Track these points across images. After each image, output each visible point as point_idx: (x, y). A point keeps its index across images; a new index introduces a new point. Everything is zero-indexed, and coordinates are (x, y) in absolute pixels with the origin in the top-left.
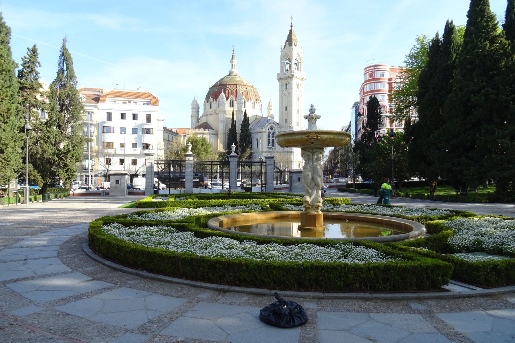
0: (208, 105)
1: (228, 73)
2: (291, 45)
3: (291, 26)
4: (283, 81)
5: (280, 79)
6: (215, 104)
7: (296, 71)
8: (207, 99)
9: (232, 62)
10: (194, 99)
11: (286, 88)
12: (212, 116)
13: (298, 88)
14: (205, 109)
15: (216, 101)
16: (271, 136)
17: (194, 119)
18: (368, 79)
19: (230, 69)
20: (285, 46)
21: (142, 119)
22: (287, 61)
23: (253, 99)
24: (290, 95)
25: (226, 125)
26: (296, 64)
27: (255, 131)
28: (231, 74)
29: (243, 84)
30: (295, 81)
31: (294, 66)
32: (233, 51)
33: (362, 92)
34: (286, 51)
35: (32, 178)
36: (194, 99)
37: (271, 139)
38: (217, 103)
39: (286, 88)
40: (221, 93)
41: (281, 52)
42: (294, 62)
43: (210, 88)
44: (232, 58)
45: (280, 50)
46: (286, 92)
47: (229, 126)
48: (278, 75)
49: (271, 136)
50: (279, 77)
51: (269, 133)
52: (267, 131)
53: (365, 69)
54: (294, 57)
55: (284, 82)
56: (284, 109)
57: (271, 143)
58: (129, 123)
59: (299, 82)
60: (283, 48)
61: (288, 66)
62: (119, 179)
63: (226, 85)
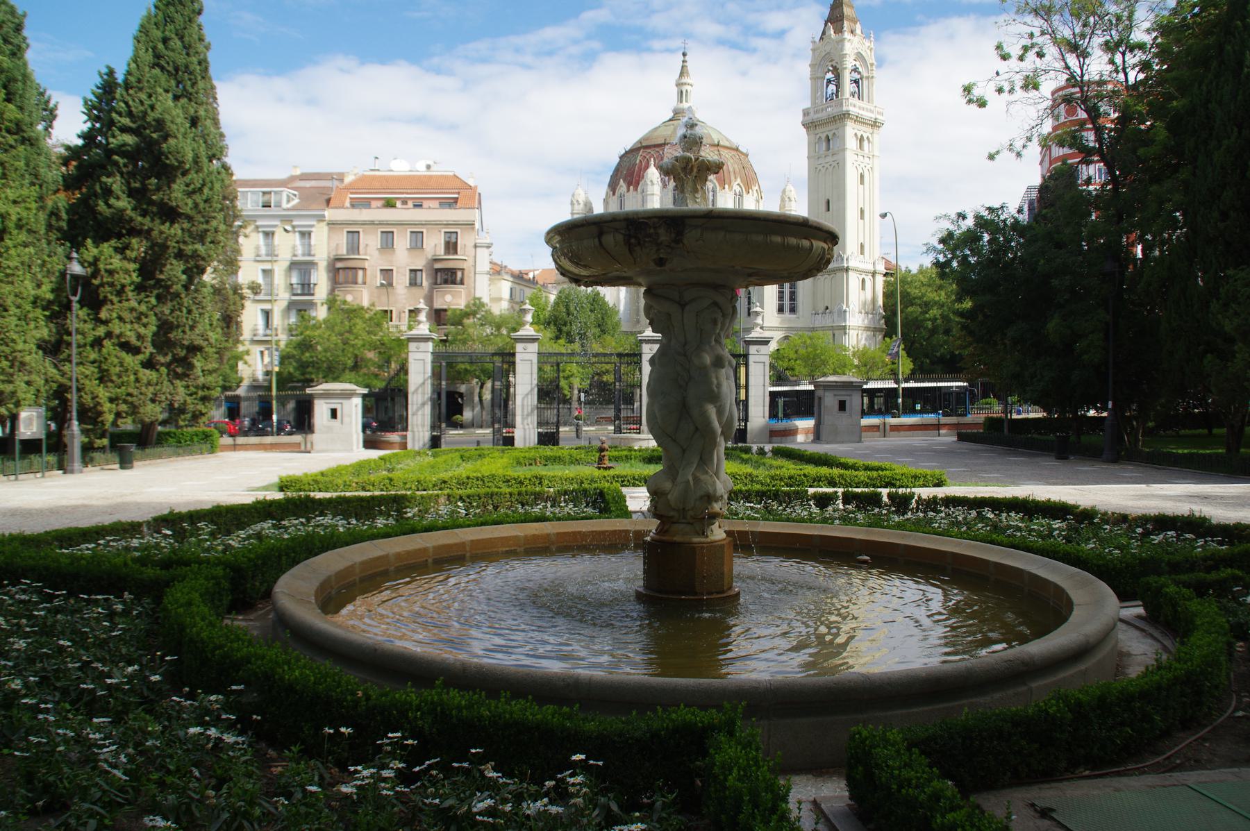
1: (671, 115)
2: (839, 30)
4: (818, 131)
5: (810, 125)
7: (855, 101)
8: (613, 186)
9: (679, 85)
11: (828, 149)
13: (861, 147)
15: (636, 189)
19: (674, 102)
20: (824, 33)
21: (434, 244)
22: (830, 75)
23: (739, 181)
24: (838, 168)
26: (856, 82)
28: (677, 113)
30: (851, 130)
31: (848, 88)
32: (684, 55)
33: (1047, 158)
34: (828, 49)
35: (87, 399)
39: (828, 149)
40: (647, 166)
41: (814, 50)
42: (847, 77)
43: (621, 157)
44: (682, 74)
45: (811, 46)
46: (829, 159)
48: (806, 113)
50: (809, 119)
53: (1053, 93)
54: (849, 63)
55: (823, 132)
56: (824, 207)
57: (787, 302)
58: (403, 259)
59: (865, 131)
60: (817, 39)
61: (832, 87)
62: (338, 407)
63: (665, 144)
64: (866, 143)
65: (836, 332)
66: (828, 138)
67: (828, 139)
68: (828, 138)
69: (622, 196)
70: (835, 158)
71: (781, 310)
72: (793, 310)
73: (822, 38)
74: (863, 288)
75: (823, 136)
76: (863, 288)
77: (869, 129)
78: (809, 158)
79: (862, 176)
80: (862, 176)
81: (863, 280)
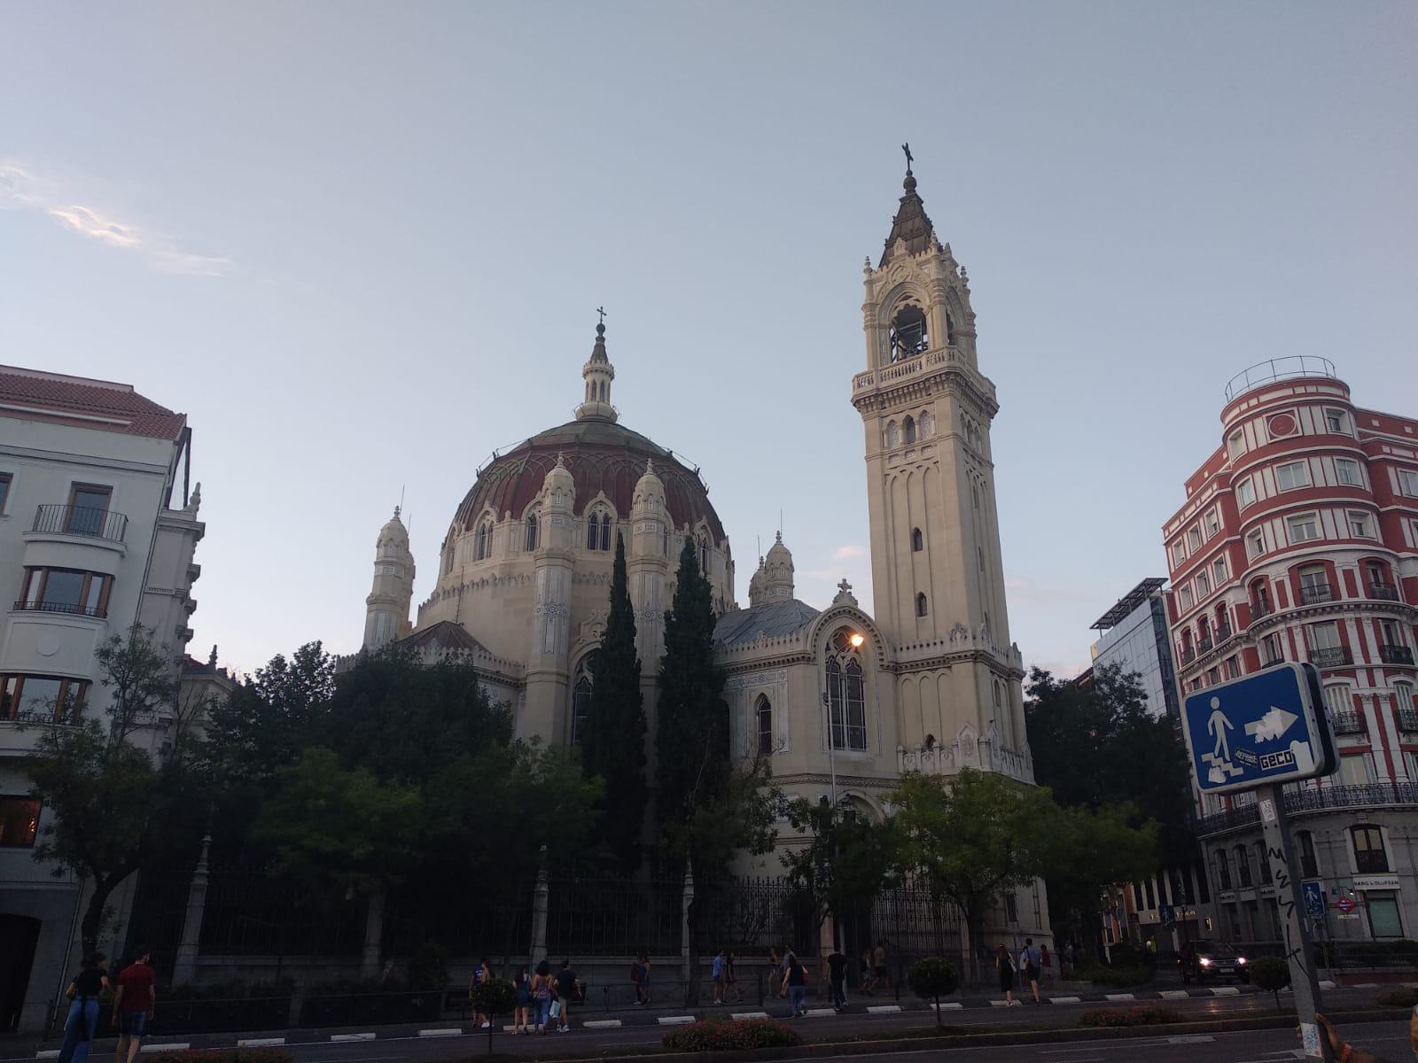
0: (466, 546)
3: (910, 184)
6: (506, 535)
8: (468, 513)
10: (397, 519)
11: (909, 438)
12: (488, 590)
14: (448, 566)
17: (382, 616)
18: (1263, 442)
25: (574, 630)
27: (748, 656)
32: (601, 328)
36: (397, 519)
38: (522, 528)
41: (870, 283)
45: (865, 277)
47: (593, 636)
50: (867, 388)
52: (822, 659)
60: (875, 266)
64: (973, 436)
66: (909, 423)
67: (909, 423)
69: (484, 535)
70: (929, 453)
72: (859, 742)
73: (885, 261)
77: (976, 415)
78: (868, 459)
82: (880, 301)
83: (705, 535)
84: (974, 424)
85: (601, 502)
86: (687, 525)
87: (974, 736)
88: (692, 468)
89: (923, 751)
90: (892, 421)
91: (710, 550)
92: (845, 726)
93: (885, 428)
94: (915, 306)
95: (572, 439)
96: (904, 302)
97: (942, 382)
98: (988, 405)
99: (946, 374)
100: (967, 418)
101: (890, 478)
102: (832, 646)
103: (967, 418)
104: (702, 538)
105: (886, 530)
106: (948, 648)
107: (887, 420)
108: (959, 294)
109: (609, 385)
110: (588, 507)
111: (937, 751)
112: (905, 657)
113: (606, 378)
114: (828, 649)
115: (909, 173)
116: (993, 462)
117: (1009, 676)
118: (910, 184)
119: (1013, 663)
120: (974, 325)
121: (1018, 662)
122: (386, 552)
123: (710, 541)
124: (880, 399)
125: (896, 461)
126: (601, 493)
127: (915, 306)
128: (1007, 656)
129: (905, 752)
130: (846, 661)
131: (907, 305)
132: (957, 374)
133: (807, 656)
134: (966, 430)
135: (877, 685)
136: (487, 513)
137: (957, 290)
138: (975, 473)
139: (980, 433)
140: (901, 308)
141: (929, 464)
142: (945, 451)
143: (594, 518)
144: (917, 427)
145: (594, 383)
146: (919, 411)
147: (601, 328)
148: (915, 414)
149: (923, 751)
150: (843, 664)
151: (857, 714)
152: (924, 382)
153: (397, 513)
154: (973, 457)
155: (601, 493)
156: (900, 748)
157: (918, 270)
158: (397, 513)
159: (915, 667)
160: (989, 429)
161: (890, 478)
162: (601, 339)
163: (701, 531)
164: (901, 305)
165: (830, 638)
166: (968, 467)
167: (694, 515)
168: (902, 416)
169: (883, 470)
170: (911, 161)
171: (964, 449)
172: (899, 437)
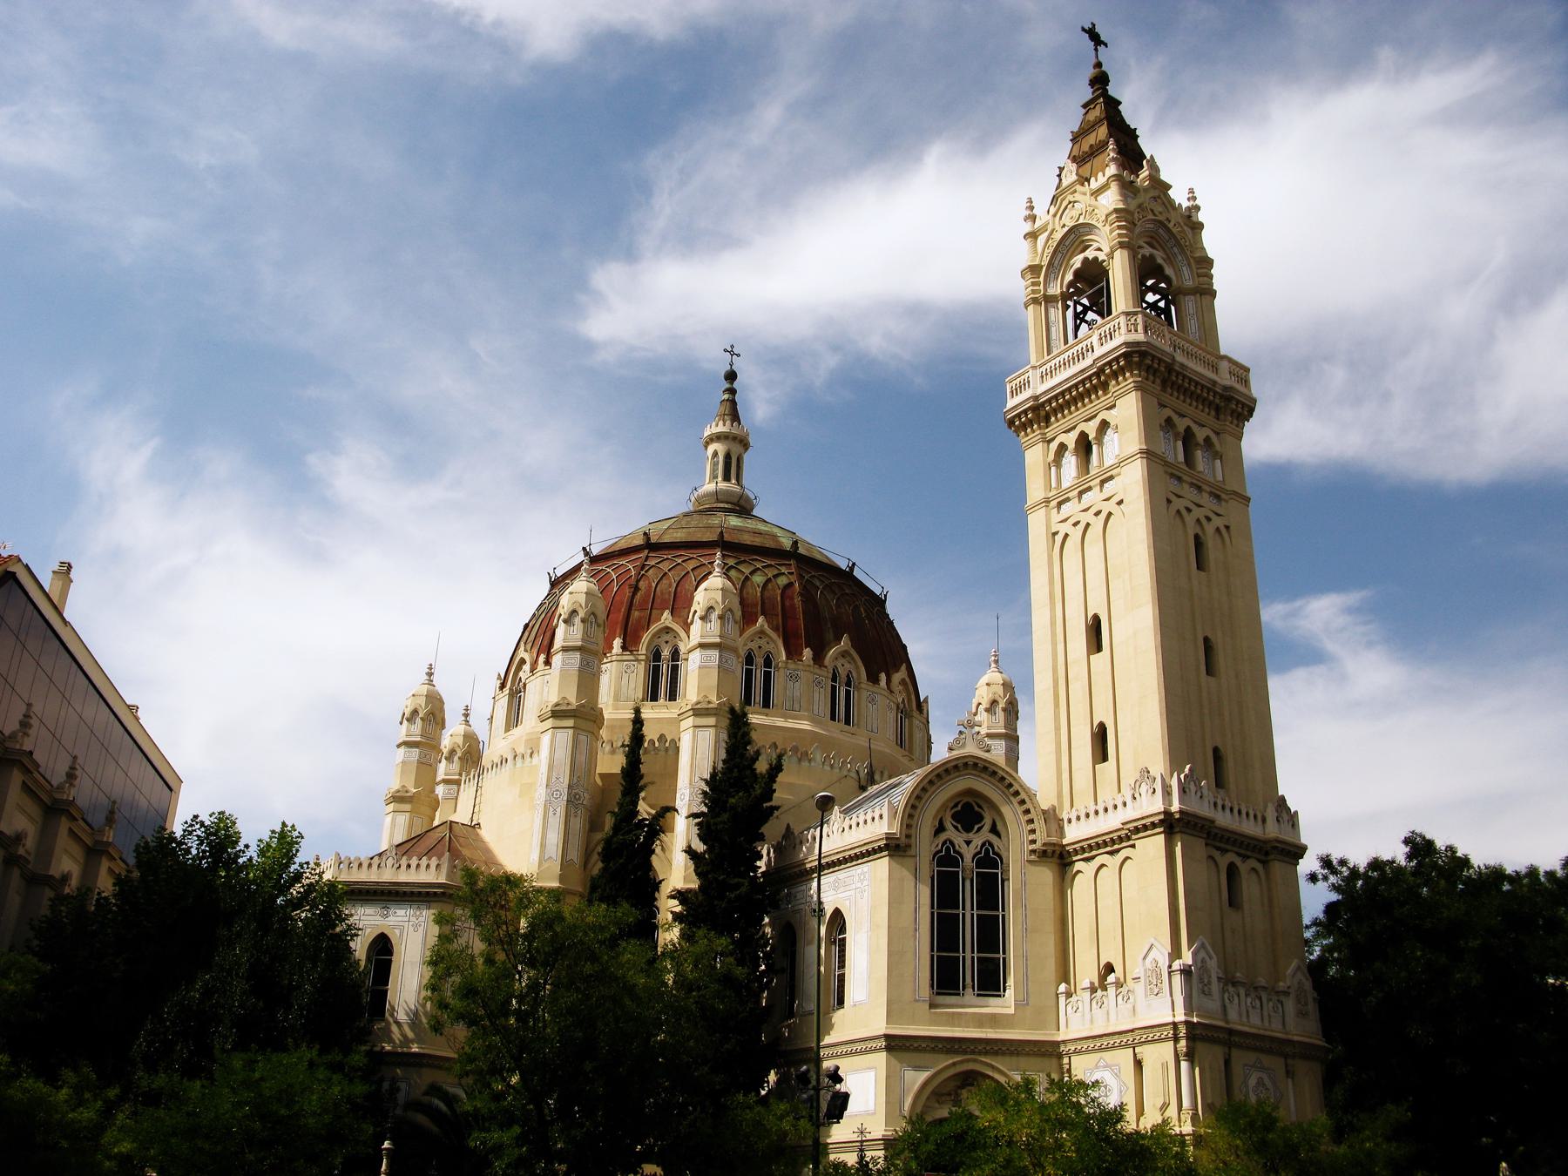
4: (1057, 425)
13: (1189, 460)
16: (968, 893)
29: (769, 544)
37: (969, 913)
49: (968, 893)
51: (947, 859)
52: (926, 846)
57: (969, 955)
64: (1199, 454)
65: (1146, 1052)
67: (1085, 447)
68: (1083, 436)
71: (946, 980)
72: (991, 982)
74: (1234, 901)
75: (1070, 439)
76: (1234, 901)
77: (1207, 417)
79: (1199, 543)
80: (1199, 543)
81: (1232, 871)
82: (1045, 262)
83: (847, 666)
84: (1200, 434)
85: (667, 630)
86: (807, 653)
87: (1164, 962)
88: (843, 565)
89: (1093, 990)
90: (1062, 447)
91: (858, 689)
92: (968, 955)
93: (1051, 456)
94: (1096, 259)
95: (639, 541)
96: (1081, 257)
97: (1122, 370)
98: (1229, 399)
99: (1124, 355)
100: (1181, 424)
101: (1059, 538)
102: (948, 823)
103: (1181, 424)
104: (842, 672)
105: (1053, 623)
106: (1132, 812)
107: (1054, 446)
108: (1175, 230)
109: (739, 460)
110: (646, 638)
111: (1111, 990)
112: (1074, 833)
113: (736, 449)
114: (941, 829)
115: (1099, 65)
116: (1249, 494)
117: (1267, 854)
118: (1100, 80)
119: (1272, 831)
120: (1211, 277)
121: (1286, 827)
122: (408, 730)
123: (859, 673)
124: (1043, 413)
125: (1067, 509)
126: (666, 614)
127: (1096, 259)
128: (1264, 820)
129: (1069, 995)
130: (973, 849)
131: (1086, 259)
132: (1143, 354)
133: (893, 843)
134: (1180, 443)
135: (1025, 886)
136: (523, 661)
137: (1171, 225)
138: (1198, 513)
139: (1218, 447)
140: (1078, 265)
141: (1110, 506)
142: (1132, 482)
143: (657, 656)
144: (1095, 448)
145: (715, 454)
146: (1095, 423)
147: (731, 376)
148: (1091, 428)
149: (1093, 990)
150: (968, 853)
151: (991, 934)
152: (1097, 374)
153: (430, 674)
154: (1199, 488)
155: (666, 614)
156: (1063, 987)
157: (1093, 202)
158: (430, 674)
159: (1092, 847)
160: (1240, 439)
161: (1059, 538)
162: (732, 391)
163: (842, 661)
164: (1077, 262)
165: (944, 806)
166: (1179, 504)
167: (830, 636)
168: (1074, 435)
169: (1048, 526)
170: (1101, 48)
171: (1172, 475)
172: (1070, 462)
